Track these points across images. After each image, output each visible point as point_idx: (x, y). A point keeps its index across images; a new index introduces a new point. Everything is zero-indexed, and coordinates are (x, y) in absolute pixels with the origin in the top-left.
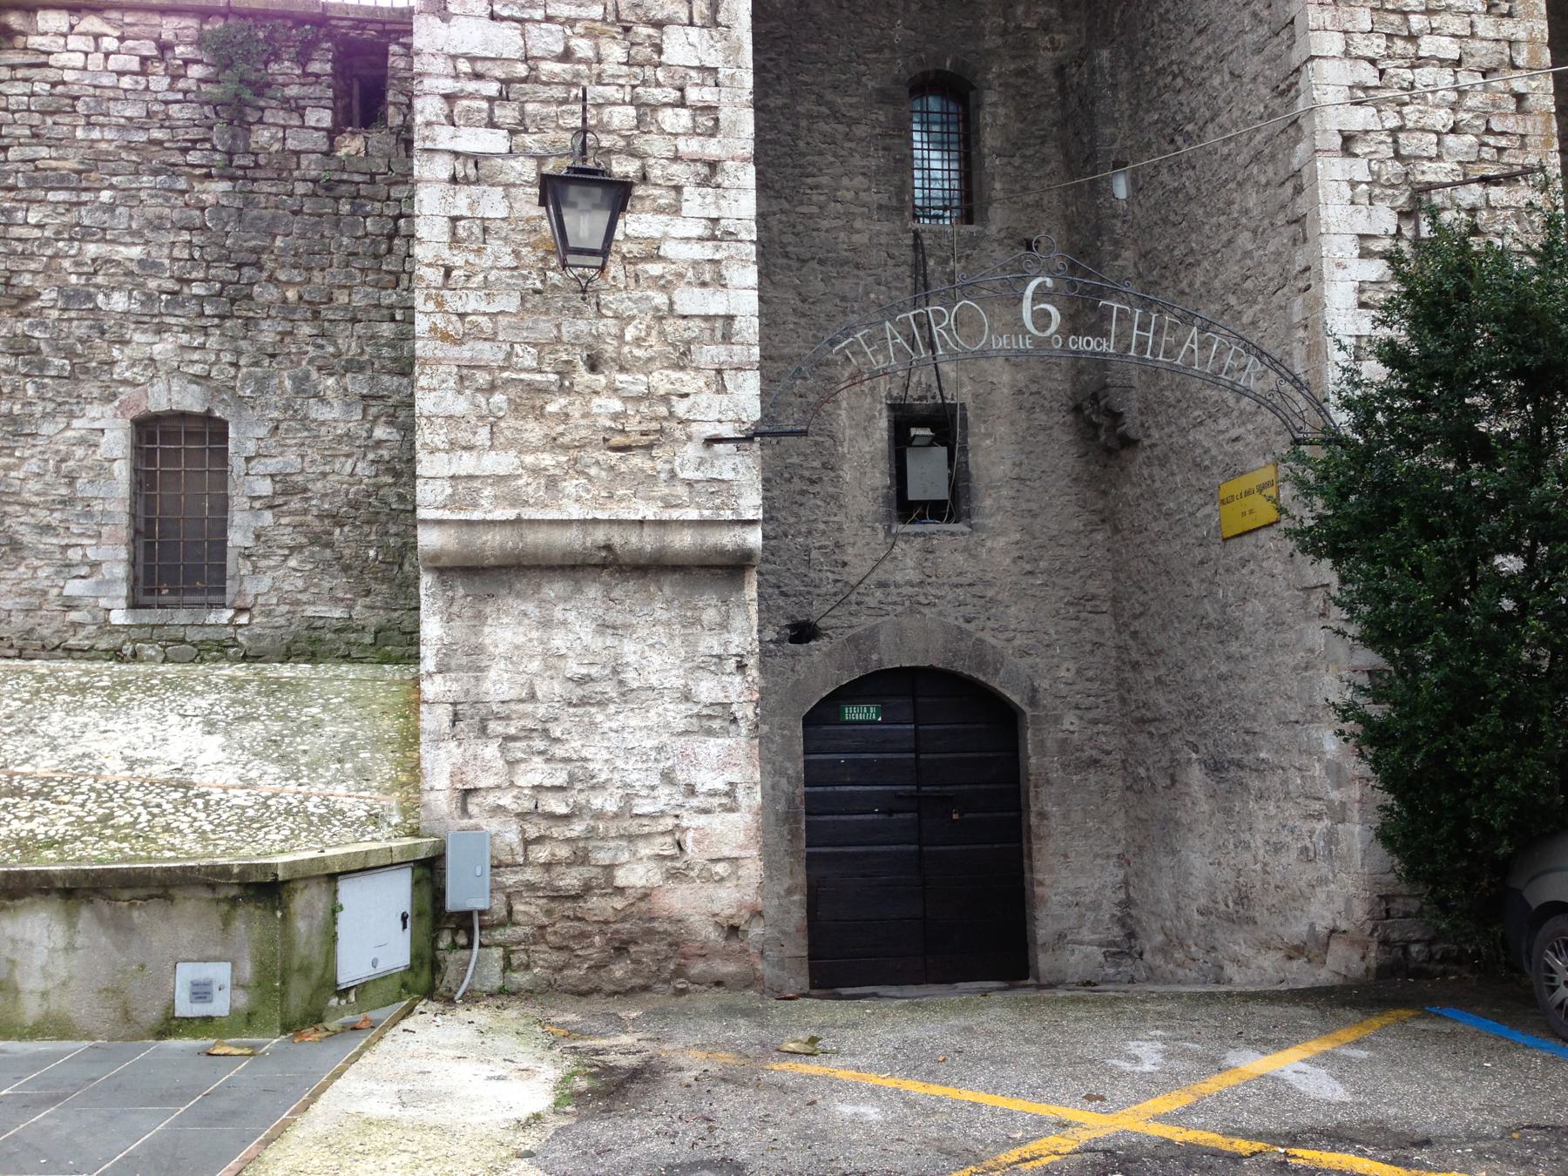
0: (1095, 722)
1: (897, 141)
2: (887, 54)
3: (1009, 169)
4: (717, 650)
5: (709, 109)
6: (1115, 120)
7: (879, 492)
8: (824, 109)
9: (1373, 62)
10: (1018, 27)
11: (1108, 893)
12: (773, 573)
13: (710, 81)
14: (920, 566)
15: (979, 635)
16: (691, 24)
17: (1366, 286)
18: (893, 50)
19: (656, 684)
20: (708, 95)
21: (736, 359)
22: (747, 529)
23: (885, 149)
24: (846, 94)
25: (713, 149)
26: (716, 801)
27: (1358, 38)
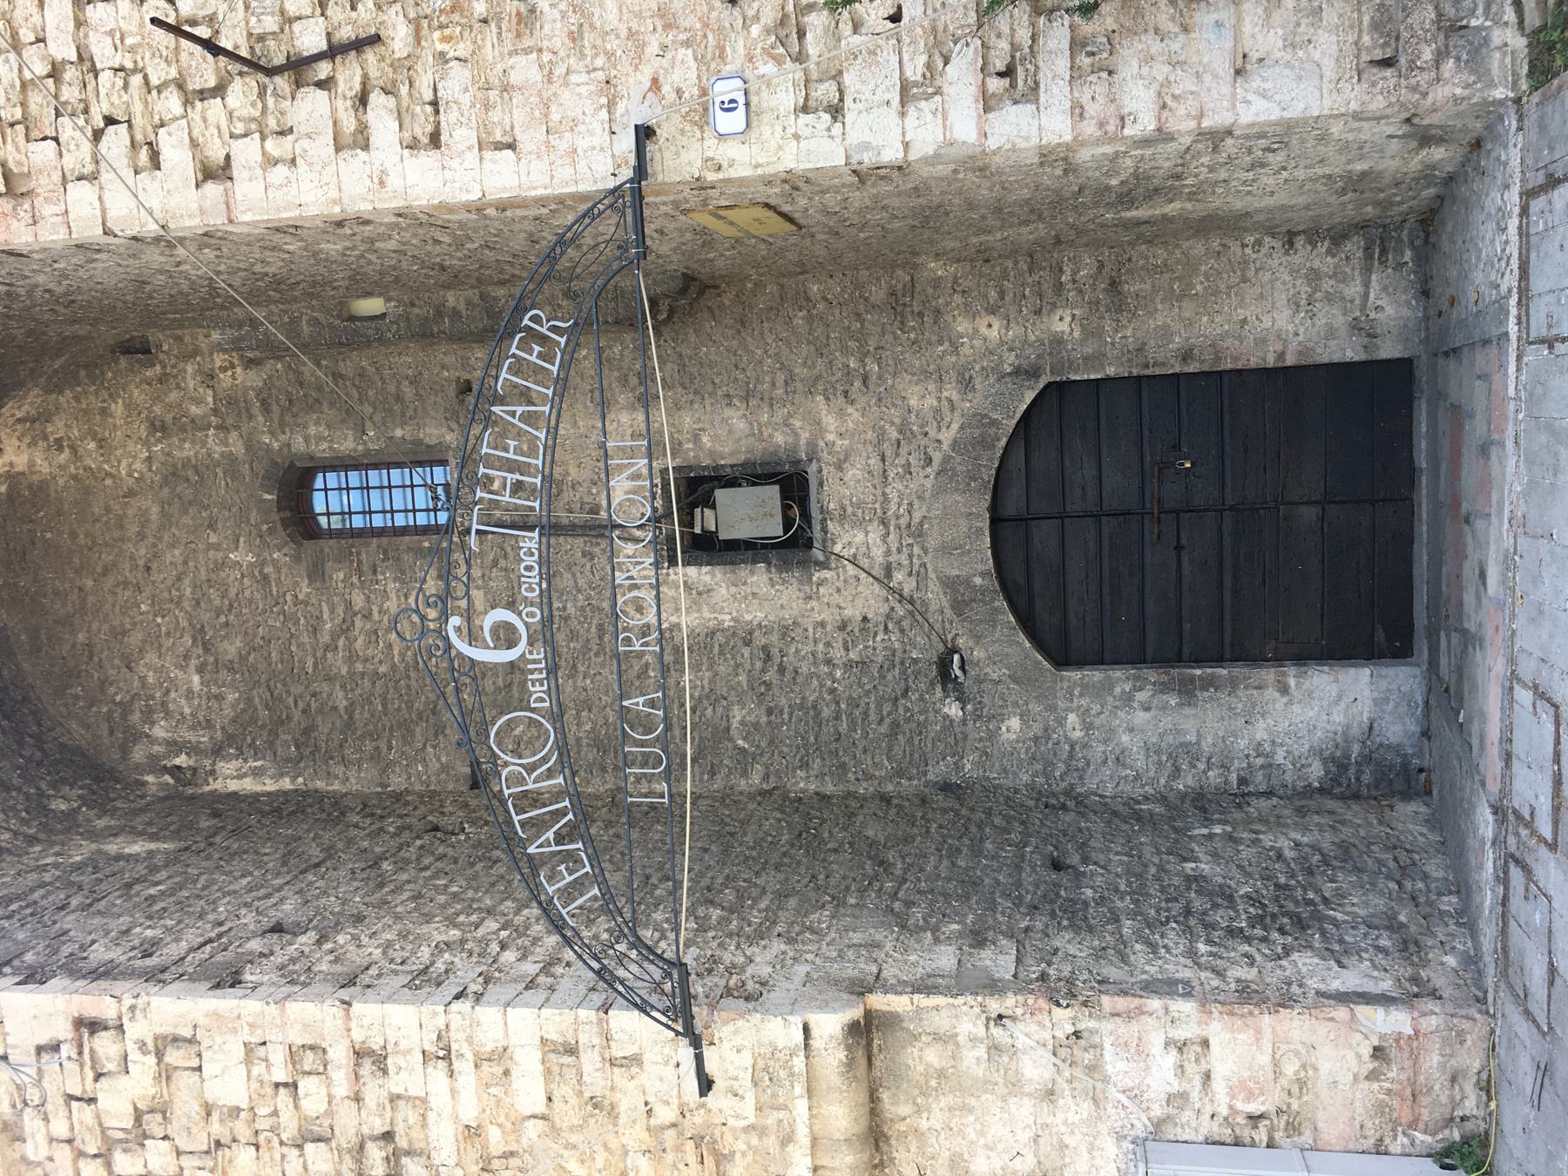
0: (1059, 287)
1: (364, 556)
2: (268, 570)
3: (377, 418)
4: (981, 1051)
5: (294, 1055)
6: (292, 321)
7: (775, 577)
8: (341, 643)
9: (97, 135)
10: (215, 411)
11: (1295, 259)
12: (879, 705)
13: (261, 1051)
14: (861, 524)
15: (945, 447)
16: (200, 1069)
17: (407, 135)
18: (263, 564)
19: (1029, 1134)
20: (278, 1056)
21: (596, 1041)
22: (815, 1032)
23: (375, 572)
24: (319, 618)
25: (339, 1054)
26: (1191, 1068)
27: (69, 161)
